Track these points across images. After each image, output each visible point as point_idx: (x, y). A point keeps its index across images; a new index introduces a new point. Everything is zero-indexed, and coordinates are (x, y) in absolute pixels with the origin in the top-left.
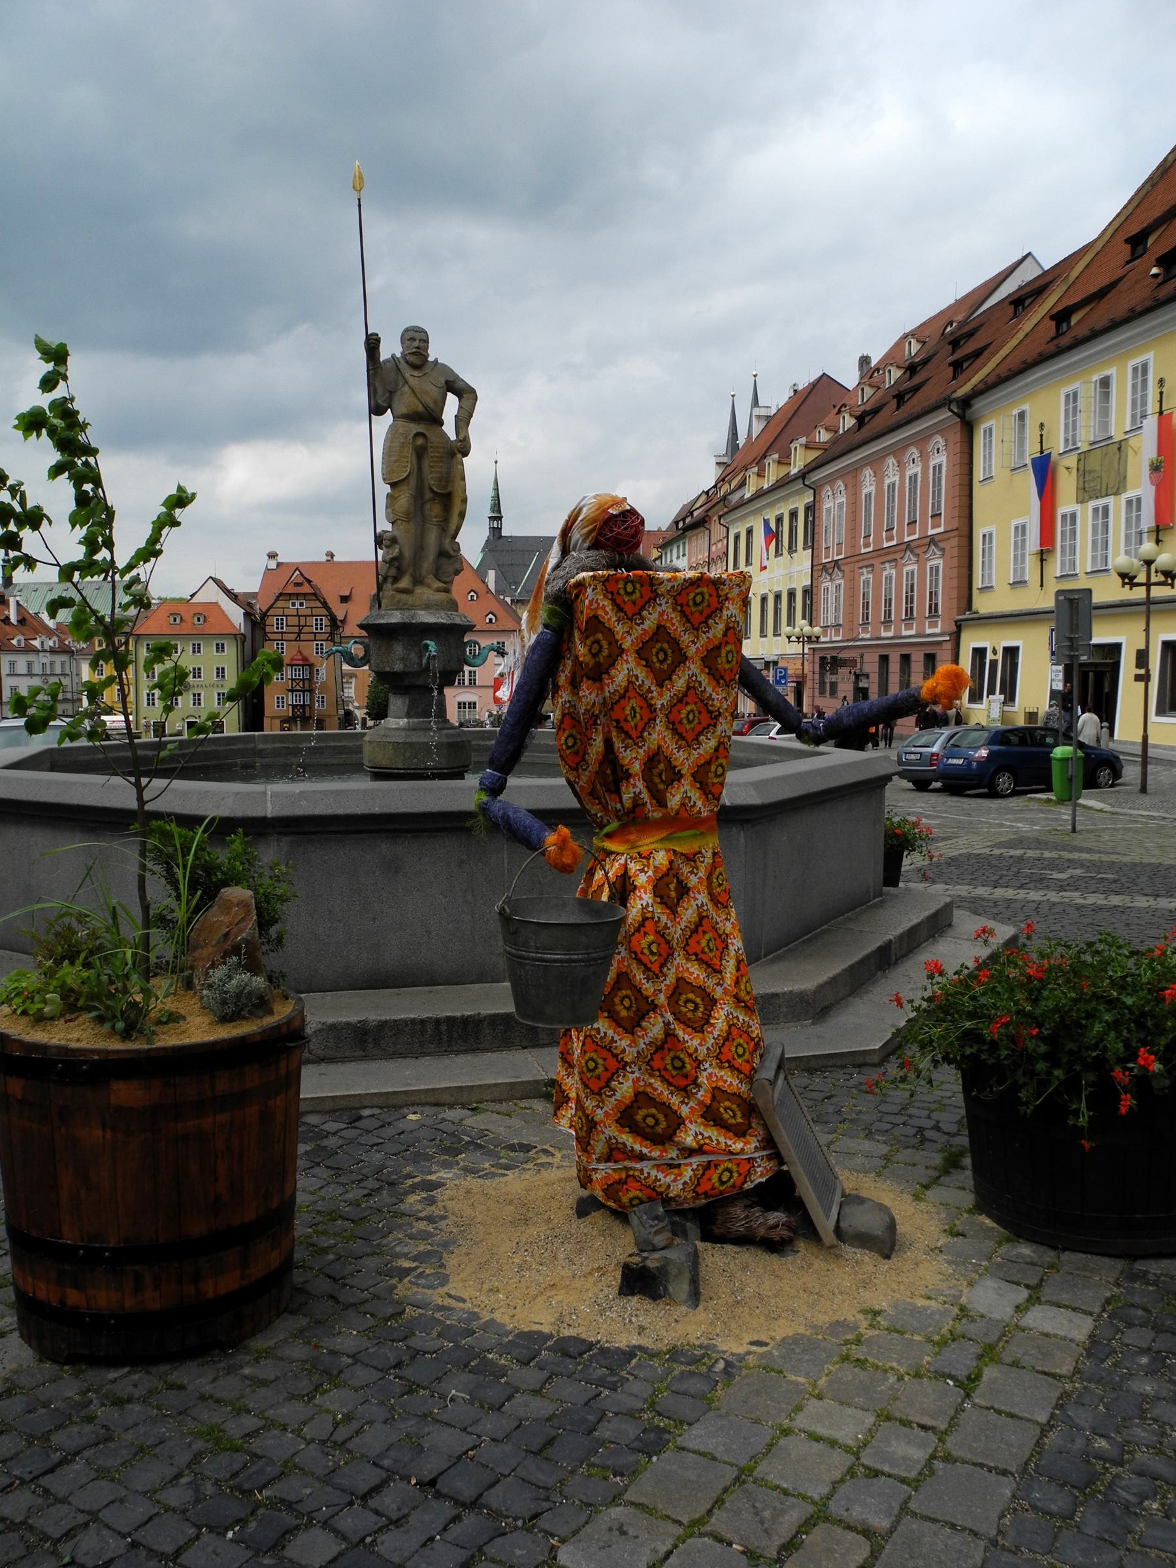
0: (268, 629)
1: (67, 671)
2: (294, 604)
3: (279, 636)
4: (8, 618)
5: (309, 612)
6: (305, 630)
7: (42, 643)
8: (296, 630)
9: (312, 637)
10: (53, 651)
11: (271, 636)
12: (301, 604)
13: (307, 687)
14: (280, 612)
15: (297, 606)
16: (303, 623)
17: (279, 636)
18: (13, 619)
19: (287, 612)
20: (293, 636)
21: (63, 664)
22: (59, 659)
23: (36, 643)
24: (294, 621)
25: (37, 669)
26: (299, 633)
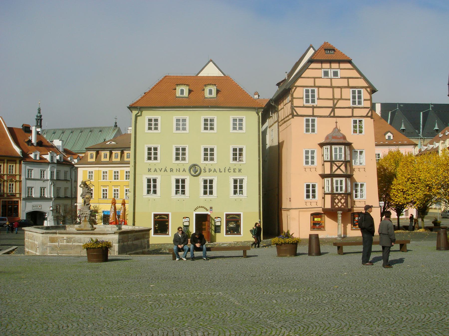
0: (296, 103)
1: (68, 178)
2: (326, 74)
3: (309, 112)
4: (30, 141)
5: (344, 83)
6: (340, 104)
7: (52, 158)
8: (330, 103)
9: (348, 112)
10: (59, 163)
11: (300, 111)
12: (335, 74)
13: (349, 173)
14: (310, 82)
15: (331, 74)
16: (337, 96)
17: (309, 112)
18: (34, 141)
19: (319, 82)
20: (327, 112)
21: (66, 173)
22: (63, 169)
23: (48, 157)
24: (326, 93)
25: (48, 175)
26: (334, 108)
